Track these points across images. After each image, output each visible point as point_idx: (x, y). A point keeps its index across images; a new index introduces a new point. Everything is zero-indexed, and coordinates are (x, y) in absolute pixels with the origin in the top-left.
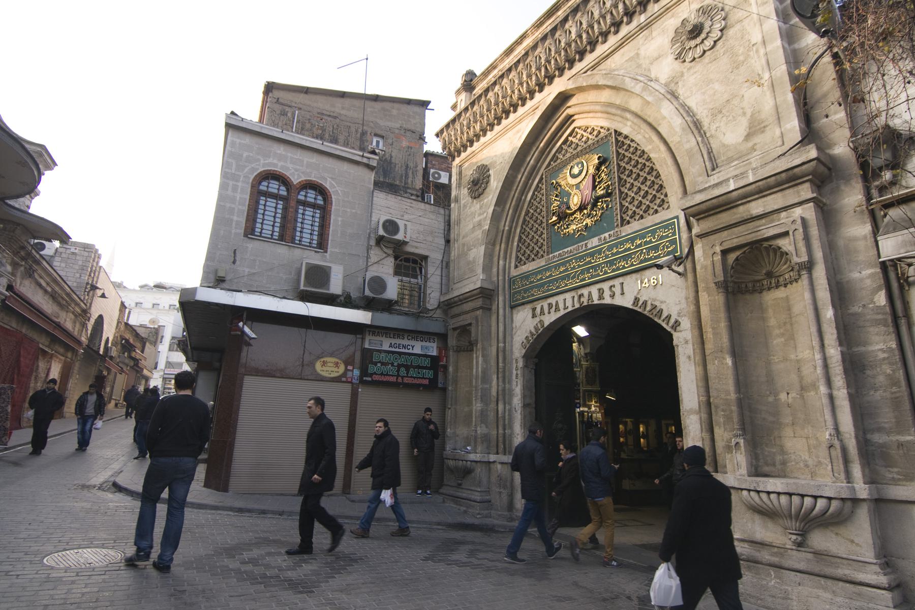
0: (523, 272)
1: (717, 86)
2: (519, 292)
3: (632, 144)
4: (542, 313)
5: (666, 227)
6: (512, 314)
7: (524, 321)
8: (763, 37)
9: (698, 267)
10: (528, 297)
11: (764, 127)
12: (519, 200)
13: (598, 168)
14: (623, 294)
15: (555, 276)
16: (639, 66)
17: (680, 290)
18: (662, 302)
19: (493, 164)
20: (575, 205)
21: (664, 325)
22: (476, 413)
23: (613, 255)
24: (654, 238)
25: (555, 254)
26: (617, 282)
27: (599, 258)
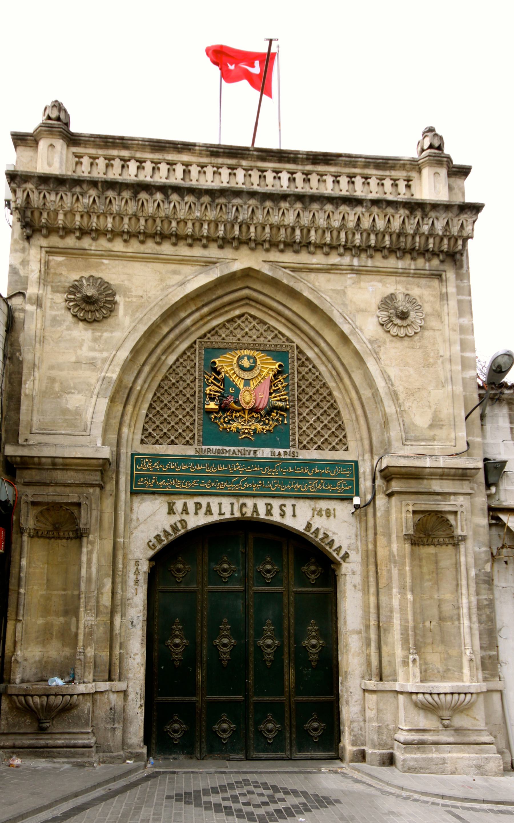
0: (156, 453)
1: (412, 371)
2: (150, 477)
3: (314, 370)
4: (185, 510)
5: (344, 466)
6: (132, 501)
7: (154, 514)
8: (450, 356)
9: (378, 514)
10: (164, 487)
11: (443, 425)
12: (159, 359)
13: (274, 376)
14: (294, 516)
15: (208, 473)
16: (344, 305)
17: (351, 527)
18: (334, 533)
19: (126, 292)
20: (248, 403)
21: (335, 554)
22: (85, 628)
23: (288, 474)
24: (333, 473)
25: (211, 447)
26: (289, 503)
27: (271, 472)
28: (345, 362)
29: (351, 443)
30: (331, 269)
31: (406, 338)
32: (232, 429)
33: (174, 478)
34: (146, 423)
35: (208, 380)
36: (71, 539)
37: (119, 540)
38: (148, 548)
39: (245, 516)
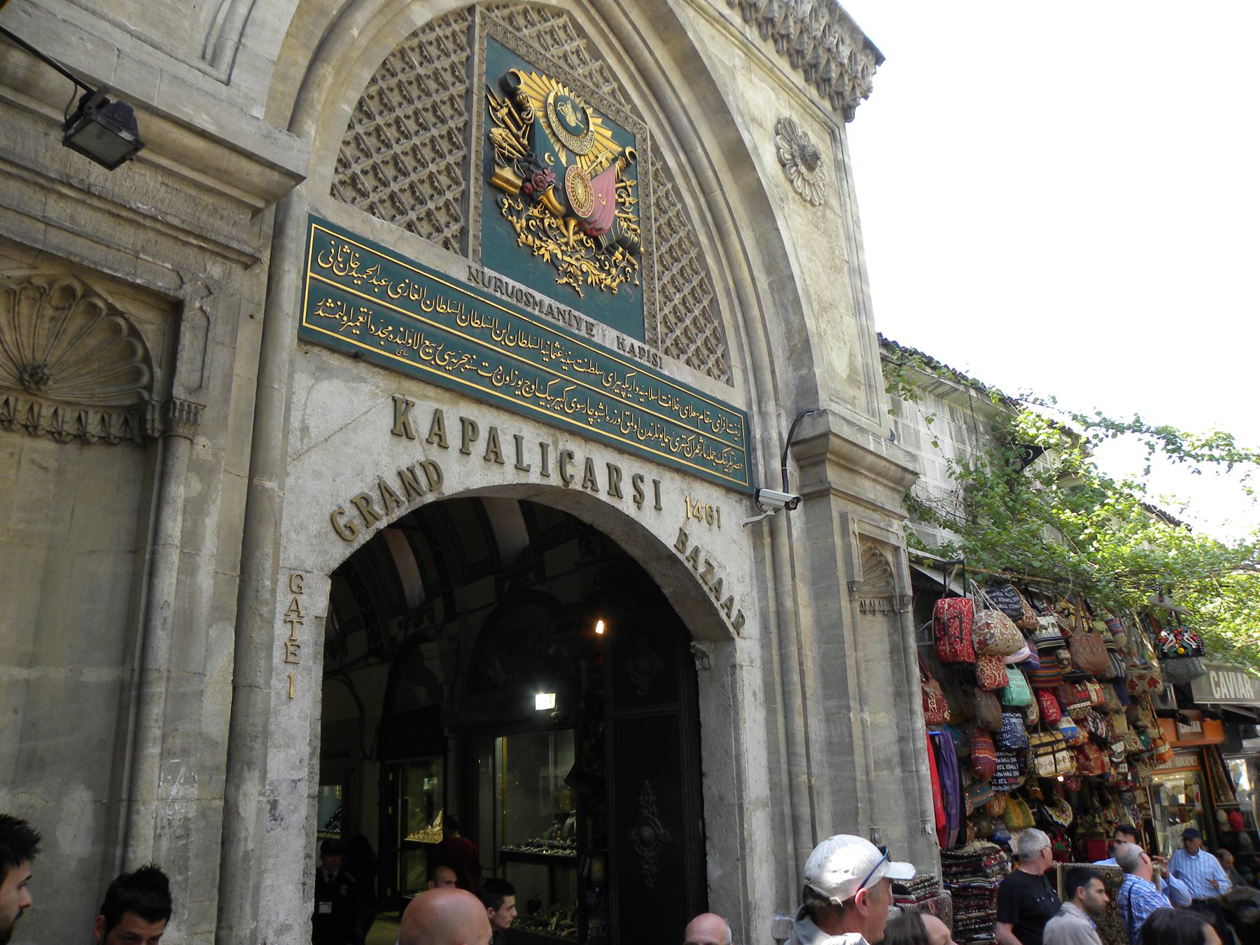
0: (371, 238)
9: (795, 534)
10: (391, 347)
18: (720, 566)
25: (505, 279)
28: (732, 205)
29: (737, 374)
30: (717, 22)
31: (808, 205)
32: (542, 251)
33: (419, 331)
34: (346, 143)
35: (495, 109)
36: (82, 438)
37: (268, 484)
38: (333, 535)
39: (571, 486)
